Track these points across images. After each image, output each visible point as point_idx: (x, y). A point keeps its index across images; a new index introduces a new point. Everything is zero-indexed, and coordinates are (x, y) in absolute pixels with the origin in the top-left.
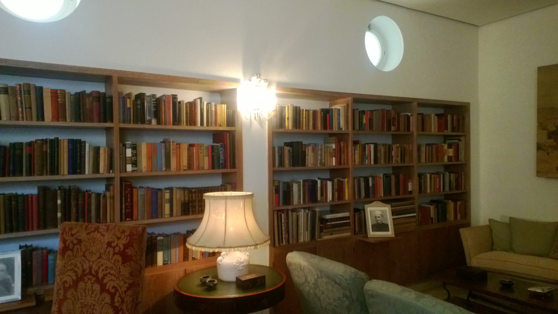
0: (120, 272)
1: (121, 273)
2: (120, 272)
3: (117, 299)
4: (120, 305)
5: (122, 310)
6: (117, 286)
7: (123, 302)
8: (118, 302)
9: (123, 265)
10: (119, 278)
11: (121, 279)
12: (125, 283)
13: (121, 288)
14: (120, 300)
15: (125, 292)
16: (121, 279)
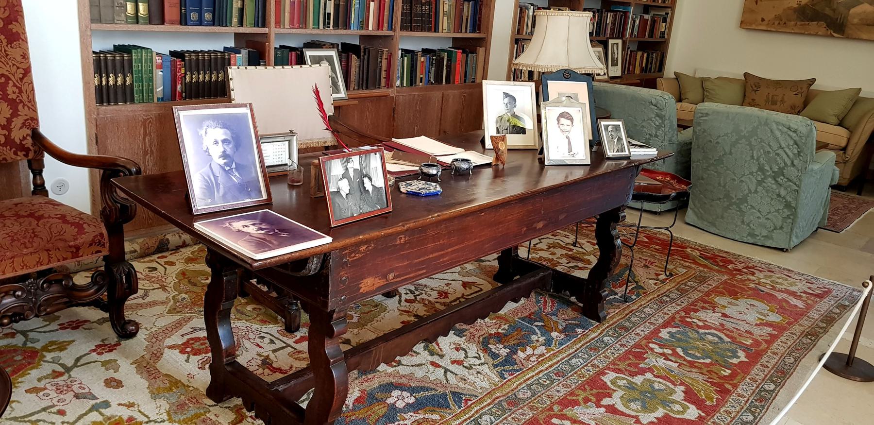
0: (7, 55)
1: (9, 57)
2: (7, 55)
3: (10, 89)
4: (18, 96)
5: (21, 101)
6: (7, 73)
7: (21, 92)
8: (14, 93)
9: (9, 46)
10: (8, 64)
11: (10, 64)
12: (18, 68)
13: (14, 76)
14: (17, 91)
15: (21, 79)
16: (10, 64)
